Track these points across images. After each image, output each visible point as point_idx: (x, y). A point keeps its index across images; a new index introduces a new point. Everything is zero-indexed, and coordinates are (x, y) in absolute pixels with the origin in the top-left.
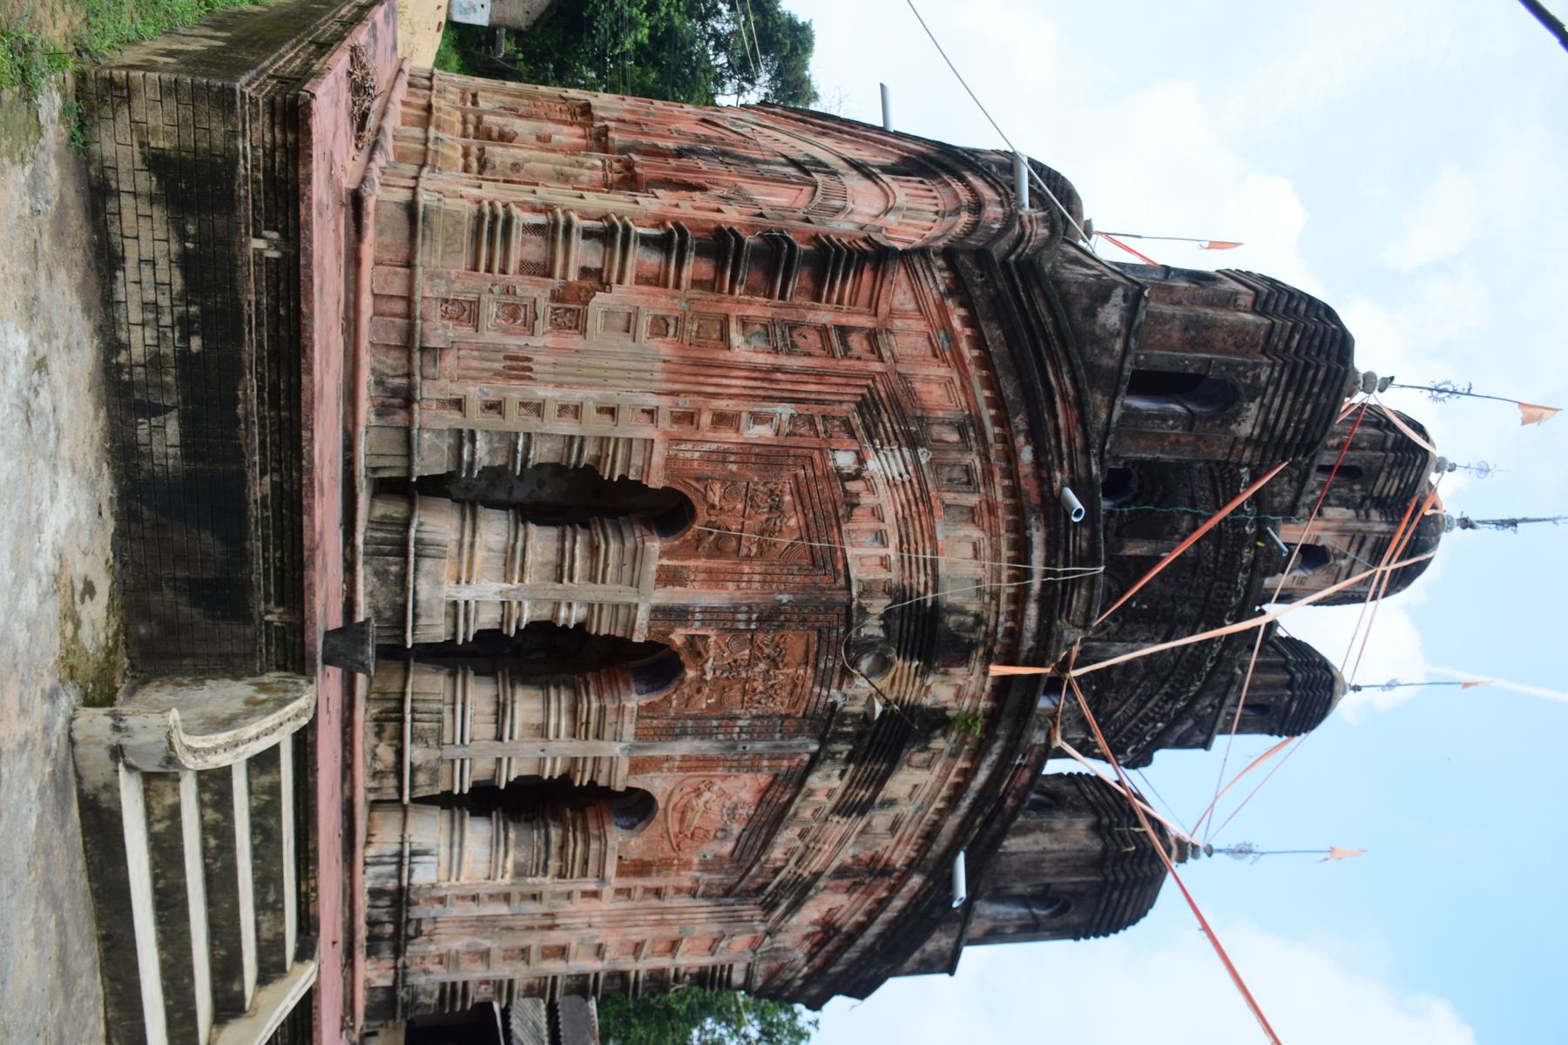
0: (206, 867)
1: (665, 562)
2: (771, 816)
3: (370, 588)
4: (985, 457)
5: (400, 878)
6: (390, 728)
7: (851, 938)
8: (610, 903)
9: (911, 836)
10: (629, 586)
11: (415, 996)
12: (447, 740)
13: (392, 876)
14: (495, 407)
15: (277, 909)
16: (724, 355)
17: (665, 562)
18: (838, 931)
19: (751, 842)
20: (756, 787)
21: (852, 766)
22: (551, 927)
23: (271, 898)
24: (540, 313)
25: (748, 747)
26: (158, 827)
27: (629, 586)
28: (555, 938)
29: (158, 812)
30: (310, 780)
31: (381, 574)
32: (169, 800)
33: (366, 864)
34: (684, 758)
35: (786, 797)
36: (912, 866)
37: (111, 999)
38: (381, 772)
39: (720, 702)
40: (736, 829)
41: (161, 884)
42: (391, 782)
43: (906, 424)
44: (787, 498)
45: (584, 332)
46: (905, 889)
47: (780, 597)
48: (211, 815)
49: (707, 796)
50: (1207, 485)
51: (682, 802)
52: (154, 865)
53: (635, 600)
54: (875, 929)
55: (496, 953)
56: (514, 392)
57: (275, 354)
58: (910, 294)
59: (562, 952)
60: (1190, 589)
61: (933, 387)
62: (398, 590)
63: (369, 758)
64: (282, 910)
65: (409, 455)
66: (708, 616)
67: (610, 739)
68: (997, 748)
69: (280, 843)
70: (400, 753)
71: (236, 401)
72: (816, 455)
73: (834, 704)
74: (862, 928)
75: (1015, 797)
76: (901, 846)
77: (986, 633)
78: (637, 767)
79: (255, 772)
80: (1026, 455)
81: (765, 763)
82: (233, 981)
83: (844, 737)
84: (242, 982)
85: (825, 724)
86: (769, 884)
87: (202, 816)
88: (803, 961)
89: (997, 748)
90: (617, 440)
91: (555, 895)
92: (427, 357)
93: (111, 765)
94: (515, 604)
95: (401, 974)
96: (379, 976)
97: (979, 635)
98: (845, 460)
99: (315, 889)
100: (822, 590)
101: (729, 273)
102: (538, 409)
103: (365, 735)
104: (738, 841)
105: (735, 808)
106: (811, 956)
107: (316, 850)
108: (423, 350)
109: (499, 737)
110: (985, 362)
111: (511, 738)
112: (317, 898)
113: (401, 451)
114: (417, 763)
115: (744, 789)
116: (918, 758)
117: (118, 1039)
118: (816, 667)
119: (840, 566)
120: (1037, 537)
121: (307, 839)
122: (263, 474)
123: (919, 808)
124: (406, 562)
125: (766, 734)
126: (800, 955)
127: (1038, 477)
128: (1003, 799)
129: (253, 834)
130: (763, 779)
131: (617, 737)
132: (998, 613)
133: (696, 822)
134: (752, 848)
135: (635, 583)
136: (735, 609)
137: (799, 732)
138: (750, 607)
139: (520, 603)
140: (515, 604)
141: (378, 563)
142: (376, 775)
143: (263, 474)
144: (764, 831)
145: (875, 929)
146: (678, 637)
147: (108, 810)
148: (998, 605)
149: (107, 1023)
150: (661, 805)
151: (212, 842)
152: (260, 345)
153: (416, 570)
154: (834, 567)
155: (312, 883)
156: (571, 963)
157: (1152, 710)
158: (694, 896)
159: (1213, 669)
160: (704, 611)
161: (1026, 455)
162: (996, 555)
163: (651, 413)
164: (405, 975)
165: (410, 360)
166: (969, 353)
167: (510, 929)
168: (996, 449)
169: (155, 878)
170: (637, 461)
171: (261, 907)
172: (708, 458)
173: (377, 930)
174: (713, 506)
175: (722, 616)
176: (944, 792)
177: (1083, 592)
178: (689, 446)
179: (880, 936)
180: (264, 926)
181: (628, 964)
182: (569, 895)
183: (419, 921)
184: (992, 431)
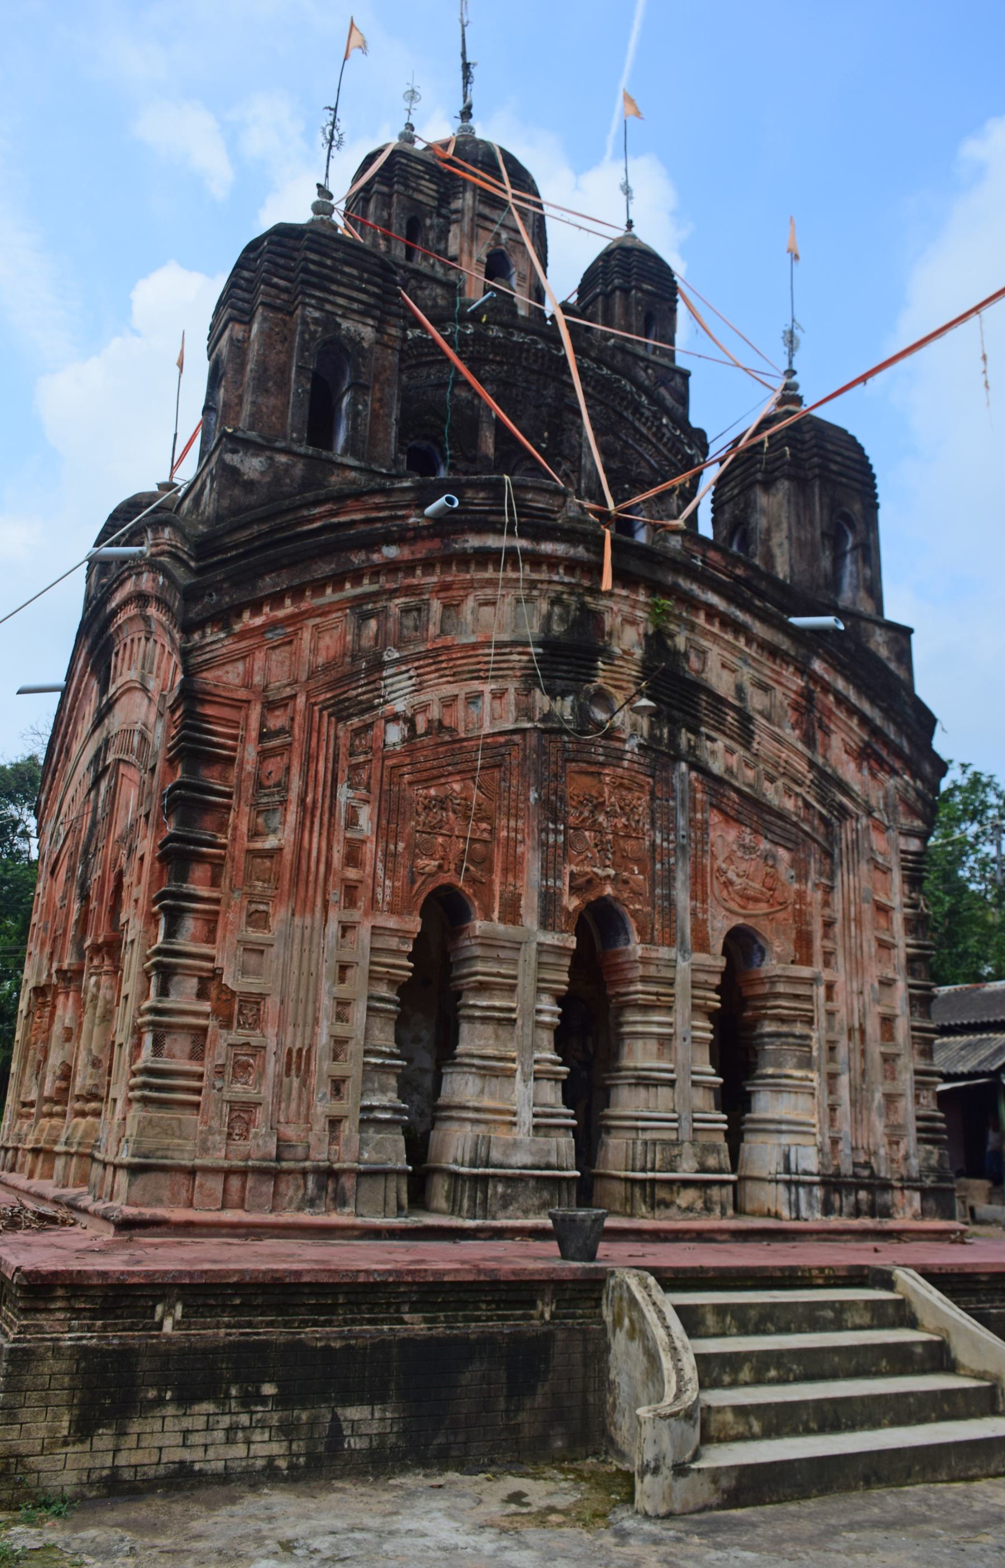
0: (798, 1379)
1: (496, 915)
2: (753, 811)
3: (519, 1213)
4: (393, 594)
5: (812, 1184)
6: (661, 1193)
7: (875, 732)
8: (839, 975)
9: (773, 670)
10: (520, 953)
11: (931, 1169)
12: (673, 1136)
13: (810, 1193)
14: (337, 1085)
15: (840, 1307)
16: (288, 855)
17: (496, 915)
18: (867, 745)
19: (778, 831)
20: (723, 825)
21: (703, 729)
22: (863, 1032)
23: (830, 1314)
24: (243, 1040)
25: (682, 833)
26: (756, 1427)
27: (520, 953)
28: (873, 1028)
29: (741, 1429)
30: (711, 1274)
31: (506, 1202)
32: (729, 1417)
33: (798, 1218)
34: (694, 897)
35: (734, 795)
36: (803, 670)
37: (929, 1476)
38: (705, 1202)
39: (638, 861)
40: (765, 845)
41: (813, 1425)
42: (715, 1192)
43: (359, 672)
44: (433, 792)
45: (262, 996)
46: (826, 677)
47: (532, 800)
48: (745, 1375)
49: (731, 875)
50: (424, 372)
51: (738, 899)
52: (795, 1433)
53: (534, 946)
54: (866, 707)
55: (889, 1087)
56: (323, 1066)
57: (281, 1309)
58: (229, 668)
59: (887, 1021)
60: (529, 389)
61: (322, 644)
62: (521, 1185)
63: (691, 1215)
64: (842, 1303)
65: (386, 1173)
66: (551, 872)
67: (673, 973)
68: (685, 584)
69: (774, 1305)
70: (686, 1184)
71: (327, 1348)
72: (389, 763)
73: (640, 746)
74: (865, 721)
75: (735, 567)
76: (783, 680)
77: (571, 594)
78: (702, 945)
79: (703, 1330)
80: (391, 552)
81: (699, 816)
82: (913, 1353)
83: (673, 736)
84: (913, 1344)
85: (660, 755)
86: (820, 813)
87: (746, 1384)
88: (898, 779)
89: (685, 584)
90: (372, 963)
91: (830, 1027)
92: (286, 1154)
93: (693, 1476)
94: (536, 1067)
95: (909, 1183)
96: (911, 1204)
97: (572, 600)
98: (394, 734)
99: (821, 1269)
100: (525, 758)
101: (205, 850)
102: (340, 1043)
103: (668, 1218)
104: (777, 844)
105: (743, 846)
106: (893, 772)
107: (782, 1269)
108: (279, 1159)
109: (671, 1083)
110: (297, 593)
111: (671, 1071)
112: (830, 1268)
113: (381, 1182)
114: (696, 1166)
115: (724, 837)
116: (695, 663)
117: (969, 1469)
118: (603, 765)
119: (502, 739)
120: (474, 541)
121: (771, 1278)
122: (402, 1322)
123: (745, 662)
124: (494, 1176)
125: (670, 815)
126: (891, 782)
127: (414, 540)
128: (737, 578)
129: (765, 1332)
130: (715, 818)
131: (672, 964)
132: (550, 582)
133: (757, 885)
134: (784, 829)
135: (517, 946)
136: (544, 845)
137: (668, 782)
138: (541, 831)
139: (536, 1062)
140: (536, 1067)
141: (494, 1205)
142: (708, 1208)
143: (402, 1322)
144: (767, 817)
145: (866, 707)
146: (572, 903)
147: (738, 1479)
148: (542, 582)
149: (953, 1480)
150: (741, 921)
151: (773, 1373)
152: (270, 1324)
153: (501, 1166)
154: (502, 745)
155: (815, 1273)
156: (898, 1012)
157: (649, 429)
158: (832, 888)
159: (609, 368)
160: (545, 876)
161: (391, 552)
162: (492, 583)
163: (346, 928)
164: (910, 1179)
165: (289, 1172)
166: (288, 608)
167: (863, 1073)
168: (385, 582)
169: (808, 1431)
170: (393, 943)
171: (839, 1325)
172: (391, 872)
173: (864, 1207)
174: (440, 867)
175: (551, 858)
176: (729, 637)
177: (530, 496)
178: (379, 890)
179: (873, 702)
180: (858, 1321)
181: (900, 954)
182: (831, 1014)
183: (855, 1165)
184: (367, 587)
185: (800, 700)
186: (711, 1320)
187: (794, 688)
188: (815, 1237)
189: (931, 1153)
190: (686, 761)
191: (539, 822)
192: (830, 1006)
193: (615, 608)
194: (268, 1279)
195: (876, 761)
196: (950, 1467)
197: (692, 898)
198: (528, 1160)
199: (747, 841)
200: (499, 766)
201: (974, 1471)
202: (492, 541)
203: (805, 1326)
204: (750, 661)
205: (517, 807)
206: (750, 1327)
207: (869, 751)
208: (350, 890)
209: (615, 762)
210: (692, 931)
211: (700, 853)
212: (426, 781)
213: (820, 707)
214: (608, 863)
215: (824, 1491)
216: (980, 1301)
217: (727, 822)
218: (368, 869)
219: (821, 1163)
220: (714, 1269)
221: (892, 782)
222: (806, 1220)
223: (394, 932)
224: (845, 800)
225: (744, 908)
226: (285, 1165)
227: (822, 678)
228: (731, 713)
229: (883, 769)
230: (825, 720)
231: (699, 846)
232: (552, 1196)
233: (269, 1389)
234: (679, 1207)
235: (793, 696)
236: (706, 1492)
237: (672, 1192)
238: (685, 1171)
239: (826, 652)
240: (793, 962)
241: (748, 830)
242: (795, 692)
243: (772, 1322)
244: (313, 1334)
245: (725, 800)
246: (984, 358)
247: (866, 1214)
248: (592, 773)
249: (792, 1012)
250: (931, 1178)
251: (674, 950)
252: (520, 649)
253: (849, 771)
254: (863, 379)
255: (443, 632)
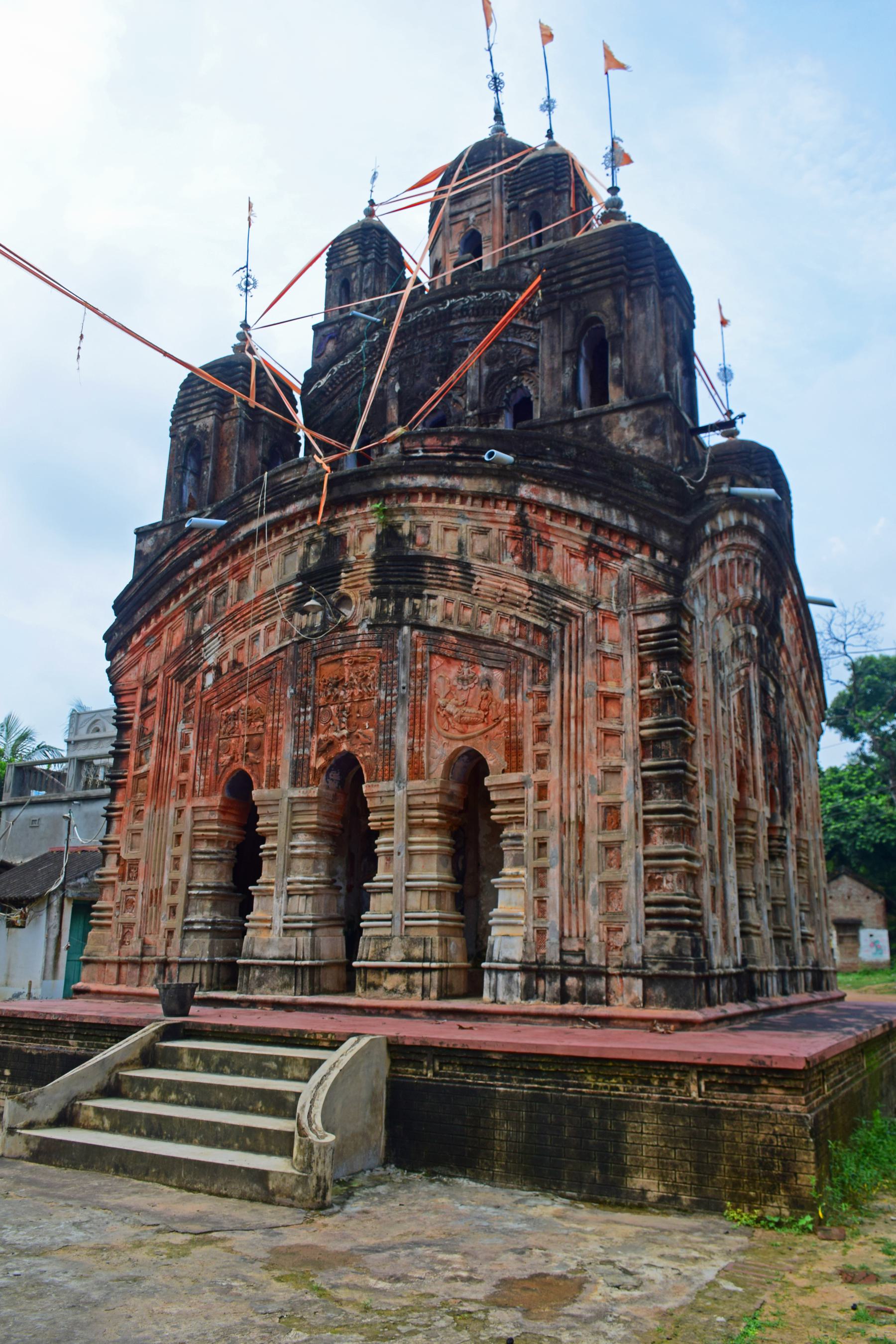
0: (190, 1104)
1: (264, 784)
2: (473, 645)
3: (269, 991)
4: (206, 588)
5: (514, 971)
6: (372, 978)
7: (598, 525)
8: (552, 774)
9: (487, 514)
10: (288, 809)
11: (663, 956)
12: (387, 932)
13: (511, 978)
14: (173, 909)
15: (283, 1062)
16: (151, 774)
17: (264, 784)
18: (590, 541)
19: (492, 655)
20: (445, 667)
21: (426, 592)
22: (581, 826)
23: (274, 1066)
24: (128, 887)
25: (403, 685)
26: (107, 1124)
27: (288, 809)
28: (593, 819)
29: (97, 1122)
30: (237, 1031)
31: (260, 982)
32: (91, 1113)
33: (495, 1002)
34: (411, 735)
35: (453, 639)
36: (512, 499)
37: (162, 1179)
38: (408, 986)
39: (369, 717)
40: (483, 672)
41: (144, 1131)
42: (417, 977)
43: (189, 647)
44: (232, 710)
45: (138, 860)
46: (534, 497)
47: (289, 696)
48: (155, 1094)
49: (450, 708)
50: (350, 388)
51: (458, 727)
52: (130, 1133)
53: (286, 800)
54: (583, 506)
55: (609, 875)
56: (167, 899)
57: (21, 1031)
58: (131, 672)
59: (611, 812)
60: (424, 352)
61: (175, 638)
62: (270, 971)
63: (395, 995)
64: (284, 1058)
65: (194, 963)
66: (301, 744)
67: (403, 800)
68: (395, 481)
69: (231, 1054)
70: (392, 970)
71: (30, 1054)
72: (205, 699)
73: (369, 627)
74: (585, 519)
75: (449, 440)
76: (497, 519)
77: (319, 532)
78: (417, 772)
79: (180, 1065)
80: (198, 564)
81: (419, 666)
82: (286, 1101)
83: (399, 608)
84: (287, 1092)
85: (384, 628)
86: (535, 626)
87: (155, 1101)
88: (631, 561)
89: (395, 481)
90: (409, 817)
91: (540, 824)
92: (147, 953)
93: (16, 1136)
94: (289, 887)
95: (627, 970)
96: (629, 992)
97: (320, 536)
98: (210, 678)
99: (325, 1034)
100: (286, 665)
101: (119, 781)
102: (175, 883)
103: (375, 997)
104: (492, 668)
105: (463, 680)
106: (624, 556)
107: (292, 1031)
108: (143, 955)
109: (390, 890)
110: (156, 612)
111: (391, 880)
112: (333, 1034)
113: (191, 968)
114: (403, 956)
115: (445, 675)
116: (421, 538)
117: (196, 1183)
118: (342, 651)
119: (271, 659)
120: (244, 531)
121: (282, 1037)
122: (68, 1044)
123: (464, 518)
124: (253, 965)
125: (393, 674)
126: (622, 567)
127: (210, 548)
128: (455, 449)
129: (222, 1073)
130: (437, 662)
131: (391, 794)
132: (301, 531)
133: (474, 710)
134: (498, 652)
135: (276, 802)
136: (296, 726)
137: (393, 648)
138: (294, 716)
139: (289, 883)
140: (289, 887)
141: (253, 984)
142: (410, 990)
143: (68, 1044)
144: (483, 647)
145: (583, 506)
146: (319, 763)
147: (40, 1145)
148: (296, 534)
149: (180, 1187)
150: (461, 744)
151: (173, 1097)
152: (15, 1039)
153: (260, 958)
154: (272, 663)
155: (319, 1036)
156: (623, 798)
157: (524, 319)
158: (548, 693)
159: (485, 291)
160: (296, 748)
161: (198, 564)
162: (262, 552)
163: (180, 812)
164: (629, 966)
165: (148, 963)
166: (153, 624)
167: (580, 863)
168: (201, 584)
169: (139, 1134)
170: (206, 815)
171: (280, 1075)
172: (204, 771)
173: (574, 994)
174: (232, 759)
175: (301, 734)
176: (445, 504)
177: (283, 477)
178: (197, 783)
179: (588, 498)
180: (297, 1074)
181: (630, 741)
182: (541, 812)
183: (562, 952)
184: (192, 591)
185: (515, 528)
186: (186, 1059)
187: (508, 520)
188: (508, 1019)
189: (666, 939)
190: (408, 625)
191: (294, 709)
192: (541, 804)
193: (352, 526)
194: (10, 1015)
195: (604, 552)
196: (179, 1176)
197: (409, 736)
198: (276, 953)
199: (466, 673)
200: (270, 678)
201: (199, 1186)
202: (255, 525)
203: (253, 1072)
204: (467, 515)
205: (279, 705)
206: (212, 1068)
207: (594, 545)
208: (182, 787)
209: (350, 646)
210: (409, 763)
211: (418, 697)
212: (227, 703)
213: (535, 526)
214: (343, 725)
215: (86, 1168)
216: (492, 1079)
217: (449, 662)
218: (191, 771)
219: (524, 953)
220: (240, 1027)
221: (625, 566)
222: (503, 1003)
223: (206, 808)
224: (568, 604)
225: (462, 733)
226: (145, 959)
227: (530, 499)
228: (453, 568)
229: (614, 557)
230: (544, 536)
231: (418, 692)
232: (291, 979)
233: (7, 1072)
234: (385, 989)
235: (508, 527)
236: (20, 1148)
237: (380, 977)
238: (392, 960)
239: (529, 475)
240: (504, 771)
241: (465, 664)
242: (510, 523)
243: (229, 1066)
244: (30, 1047)
245: (443, 645)
246: (82, 337)
247: (576, 1000)
248: (336, 661)
249: (504, 816)
250: (660, 966)
251: (392, 782)
252: (286, 589)
253: (580, 576)
254: (166, 354)
255: (239, 599)
